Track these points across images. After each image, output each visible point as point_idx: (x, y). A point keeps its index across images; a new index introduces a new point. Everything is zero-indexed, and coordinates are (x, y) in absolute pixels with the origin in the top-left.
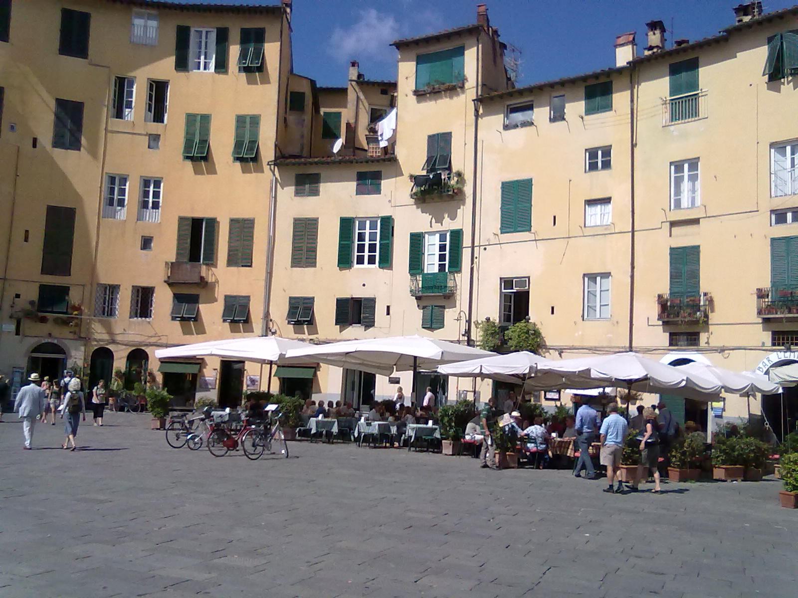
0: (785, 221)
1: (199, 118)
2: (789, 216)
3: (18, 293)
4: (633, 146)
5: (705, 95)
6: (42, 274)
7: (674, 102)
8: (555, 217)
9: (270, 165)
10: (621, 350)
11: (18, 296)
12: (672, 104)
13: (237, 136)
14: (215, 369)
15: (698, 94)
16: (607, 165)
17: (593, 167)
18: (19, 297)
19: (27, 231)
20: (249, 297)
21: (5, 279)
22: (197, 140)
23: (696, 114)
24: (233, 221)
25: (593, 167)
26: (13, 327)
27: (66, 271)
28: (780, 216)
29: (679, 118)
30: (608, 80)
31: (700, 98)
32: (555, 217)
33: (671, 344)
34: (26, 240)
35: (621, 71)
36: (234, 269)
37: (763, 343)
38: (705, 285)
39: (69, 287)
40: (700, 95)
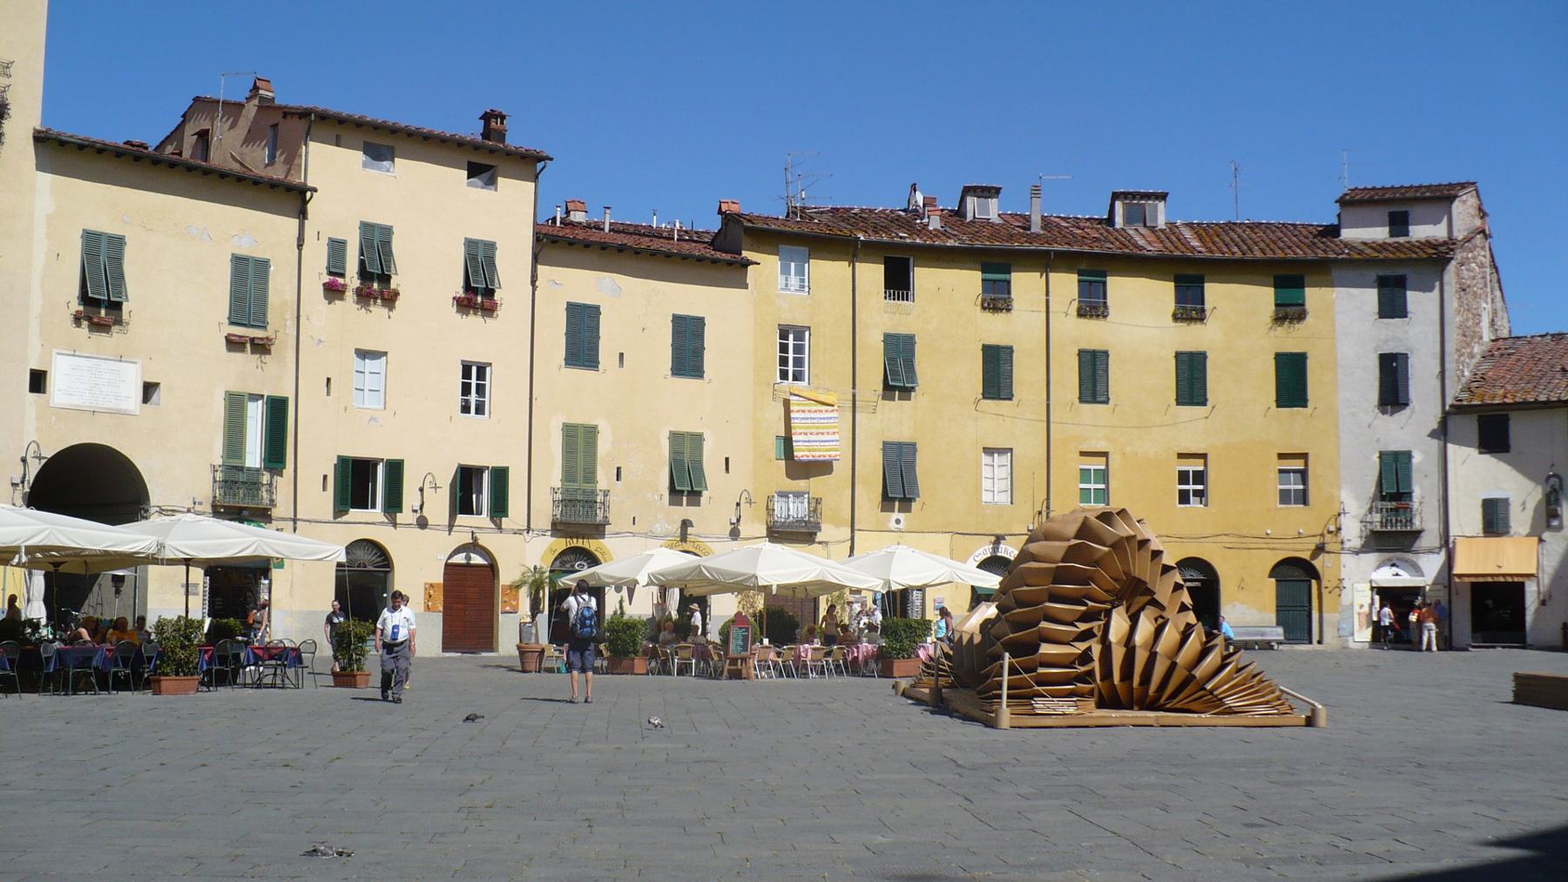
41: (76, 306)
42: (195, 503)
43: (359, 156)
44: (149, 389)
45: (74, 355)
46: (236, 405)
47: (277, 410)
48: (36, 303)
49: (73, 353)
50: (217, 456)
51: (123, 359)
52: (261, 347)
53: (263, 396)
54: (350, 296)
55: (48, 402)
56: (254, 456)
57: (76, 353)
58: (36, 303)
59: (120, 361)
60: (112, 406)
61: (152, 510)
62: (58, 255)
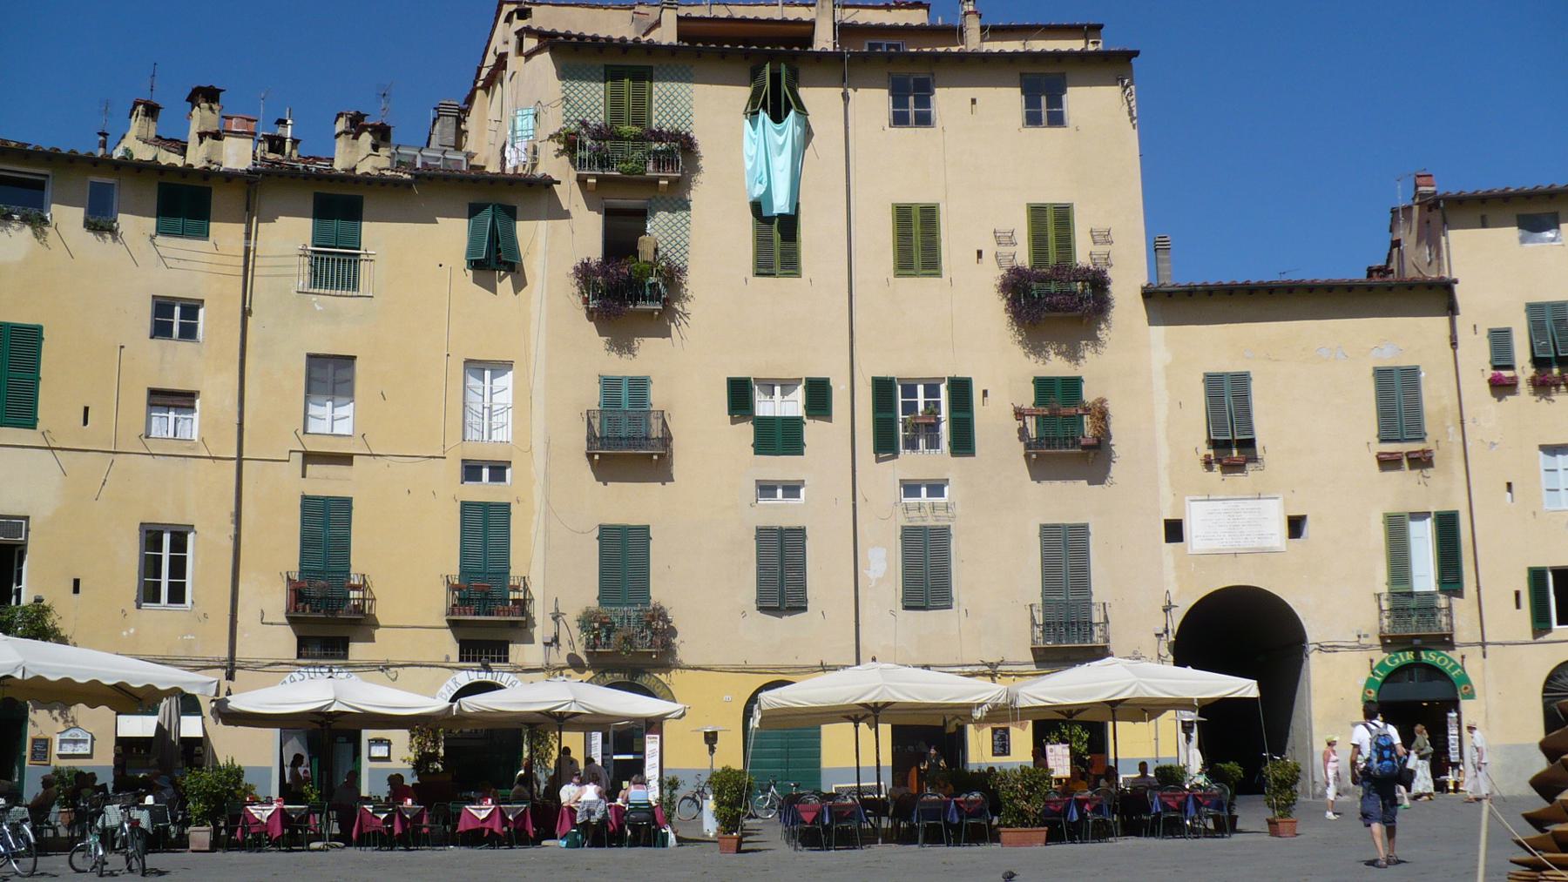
0: (479, 478)
2: (486, 472)
4: (246, 313)
5: (371, 260)
7: (320, 256)
8: (86, 409)
10: (212, 664)
12: (316, 259)
15: (359, 254)
16: (189, 332)
17: (161, 330)
23: (355, 287)
25: (161, 330)
28: (471, 471)
29: (332, 285)
30: (206, 184)
31: (362, 263)
32: (86, 409)
33: (299, 656)
35: (230, 177)
37: (448, 658)
38: (359, 564)
40: (362, 257)
41: (1205, 450)
42: (1359, 636)
43: (1513, 233)
44: (1296, 526)
45: (1208, 500)
46: (1396, 528)
47: (1447, 526)
48: (1164, 454)
49: (1206, 498)
50: (1380, 581)
51: (1261, 496)
52: (1421, 461)
53: (1429, 513)
54: (1524, 387)
55: (1186, 549)
56: (1425, 577)
57: (1210, 498)
58: (1164, 454)
59: (1259, 498)
60: (1255, 545)
61: (1311, 648)
62: (1180, 404)
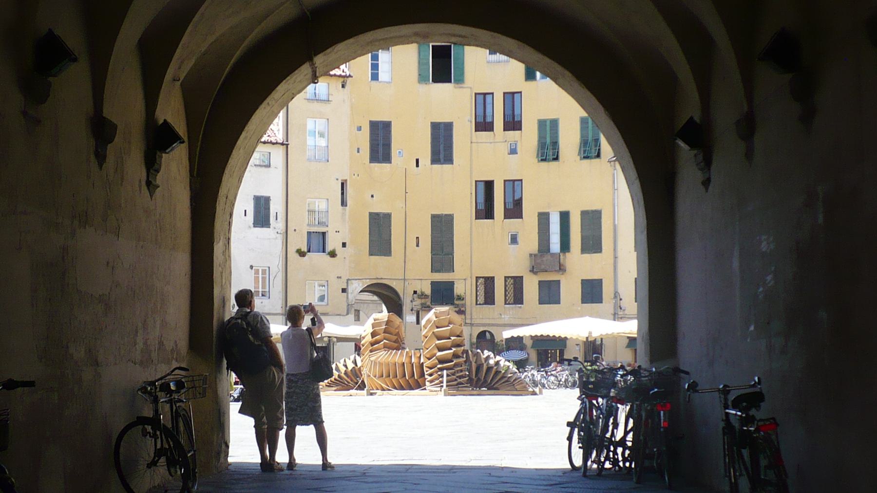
1: (548, 123)
3: (415, 290)
6: (432, 272)
9: (610, 162)
11: (415, 292)
13: (582, 136)
14: (577, 345)
18: (416, 291)
19: (417, 238)
20: (601, 280)
21: (404, 279)
22: (548, 141)
24: (584, 214)
26: (414, 318)
27: (451, 269)
34: (418, 245)
36: (587, 256)
39: (454, 282)
